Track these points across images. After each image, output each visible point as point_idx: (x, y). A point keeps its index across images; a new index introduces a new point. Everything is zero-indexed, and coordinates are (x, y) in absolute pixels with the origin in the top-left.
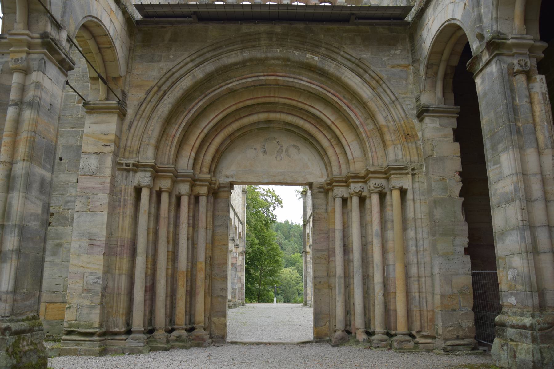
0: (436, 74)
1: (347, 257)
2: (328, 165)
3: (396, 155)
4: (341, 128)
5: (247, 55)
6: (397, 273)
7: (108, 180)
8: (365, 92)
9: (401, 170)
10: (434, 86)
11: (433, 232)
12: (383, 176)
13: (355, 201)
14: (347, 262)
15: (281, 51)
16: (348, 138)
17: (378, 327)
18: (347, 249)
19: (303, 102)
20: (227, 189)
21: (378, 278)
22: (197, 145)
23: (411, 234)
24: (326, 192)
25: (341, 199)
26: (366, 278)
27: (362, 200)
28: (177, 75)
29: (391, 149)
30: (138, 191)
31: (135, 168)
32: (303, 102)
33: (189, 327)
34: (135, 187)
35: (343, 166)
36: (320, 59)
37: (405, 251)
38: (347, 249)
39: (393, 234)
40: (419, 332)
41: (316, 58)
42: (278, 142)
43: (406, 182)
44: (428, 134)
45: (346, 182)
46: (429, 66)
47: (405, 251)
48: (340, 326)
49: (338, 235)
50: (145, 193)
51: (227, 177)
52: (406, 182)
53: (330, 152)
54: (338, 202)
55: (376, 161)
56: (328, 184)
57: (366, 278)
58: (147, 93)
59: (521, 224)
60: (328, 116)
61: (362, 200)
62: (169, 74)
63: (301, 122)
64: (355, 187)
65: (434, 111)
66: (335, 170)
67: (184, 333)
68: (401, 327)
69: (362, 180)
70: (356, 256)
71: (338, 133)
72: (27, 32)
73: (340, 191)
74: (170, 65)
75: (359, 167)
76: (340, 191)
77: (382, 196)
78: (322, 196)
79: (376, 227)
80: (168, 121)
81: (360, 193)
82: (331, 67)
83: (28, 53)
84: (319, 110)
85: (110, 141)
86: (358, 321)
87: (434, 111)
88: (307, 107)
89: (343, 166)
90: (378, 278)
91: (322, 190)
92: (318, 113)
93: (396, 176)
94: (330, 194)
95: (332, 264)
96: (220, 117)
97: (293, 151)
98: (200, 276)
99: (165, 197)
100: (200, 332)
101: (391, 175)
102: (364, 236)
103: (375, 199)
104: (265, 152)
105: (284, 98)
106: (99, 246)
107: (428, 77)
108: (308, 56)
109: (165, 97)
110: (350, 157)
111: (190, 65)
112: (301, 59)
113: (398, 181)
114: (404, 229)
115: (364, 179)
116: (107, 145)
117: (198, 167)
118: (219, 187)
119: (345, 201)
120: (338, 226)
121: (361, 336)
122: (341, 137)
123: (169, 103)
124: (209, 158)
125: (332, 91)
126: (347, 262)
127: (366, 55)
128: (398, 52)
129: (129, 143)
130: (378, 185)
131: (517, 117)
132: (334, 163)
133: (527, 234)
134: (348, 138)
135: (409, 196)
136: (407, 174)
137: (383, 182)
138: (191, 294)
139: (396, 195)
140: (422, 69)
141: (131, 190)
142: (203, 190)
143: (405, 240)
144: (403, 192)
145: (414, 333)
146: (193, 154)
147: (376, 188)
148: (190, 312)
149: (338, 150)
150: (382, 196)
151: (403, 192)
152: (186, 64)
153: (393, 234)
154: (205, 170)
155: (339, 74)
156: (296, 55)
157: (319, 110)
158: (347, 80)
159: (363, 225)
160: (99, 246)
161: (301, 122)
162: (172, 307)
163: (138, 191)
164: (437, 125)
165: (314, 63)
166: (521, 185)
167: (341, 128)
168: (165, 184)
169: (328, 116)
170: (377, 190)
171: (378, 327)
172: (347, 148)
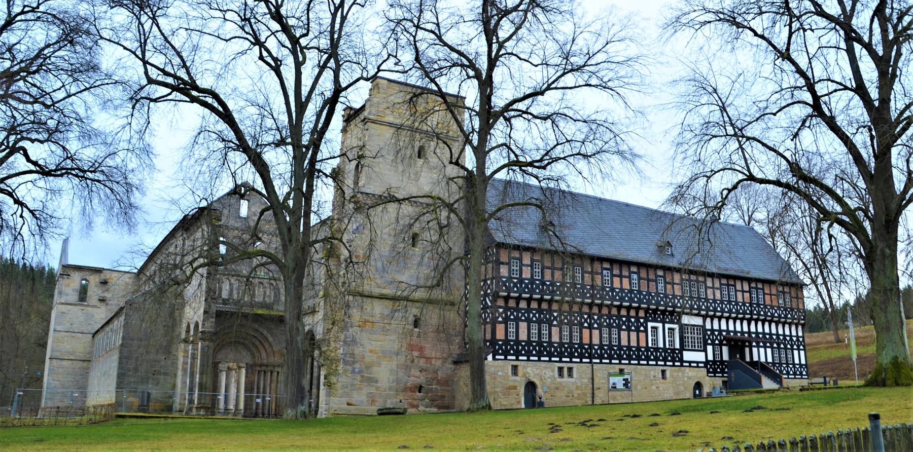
17: (266, 412)
23: (279, 385)
27: (265, 372)
37: (277, 389)
39: (273, 385)
43: (279, 370)
45: (261, 366)
47: (277, 389)
48: (254, 412)
49: (256, 383)
60: (257, 343)
61: (265, 372)
64: (263, 368)
68: (273, 412)
73: (258, 368)
75: (265, 362)
76: (258, 368)
77: (272, 372)
79: (269, 382)
82: (261, 330)
86: (260, 411)
102: (264, 384)
103: (269, 373)
113: (277, 369)
114: (277, 383)
115: (267, 366)
119: (259, 371)
120: (256, 380)
121: (261, 415)
139: (276, 373)
143: (277, 387)
144: (278, 372)
150: (272, 372)
151: (278, 372)
153: (273, 385)
159: (264, 381)
167: (261, 348)
169: (257, 343)
171: (266, 412)
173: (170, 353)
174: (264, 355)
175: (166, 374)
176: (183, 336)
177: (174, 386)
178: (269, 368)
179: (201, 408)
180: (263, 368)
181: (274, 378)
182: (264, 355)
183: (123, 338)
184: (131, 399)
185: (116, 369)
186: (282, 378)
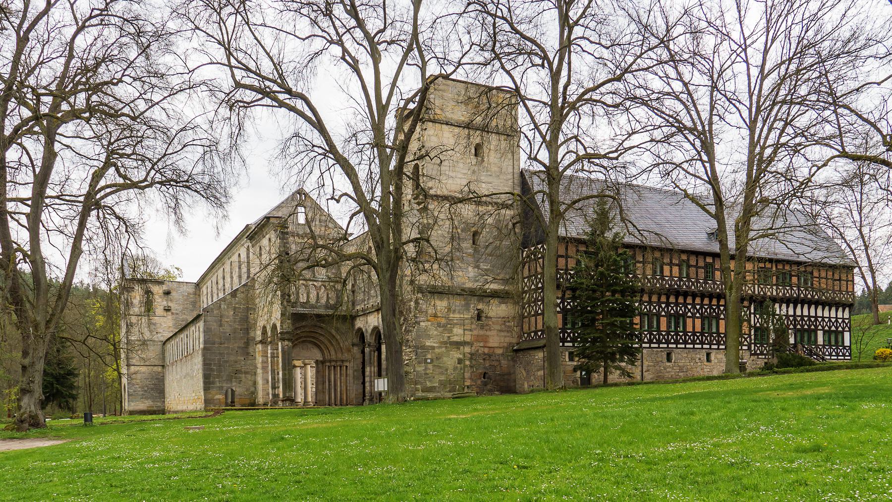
2: (323, 354)
4: (328, 345)
6: (344, 388)
9: (346, 361)
11: (354, 378)
14: (329, 385)
16: (331, 349)
18: (330, 381)
21: (339, 390)
26: (335, 390)
38: (330, 381)
43: (347, 364)
44: (355, 351)
45: (330, 361)
52: (347, 364)
57: (335, 390)
64: (333, 364)
73: (328, 364)
75: (334, 357)
86: (333, 401)
90: (339, 390)
115: (336, 361)
120: (327, 374)
126: (329, 385)
134: (331, 349)
140: (354, 332)
144: (347, 367)
150: (341, 367)
159: (335, 375)
173: (248, 354)
174: (333, 352)
175: (246, 373)
176: (259, 338)
177: (255, 383)
178: (338, 363)
179: (286, 400)
180: (333, 364)
181: (344, 372)
182: (333, 352)
183: (205, 342)
184: (218, 397)
185: (201, 371)
186: (350, 372)
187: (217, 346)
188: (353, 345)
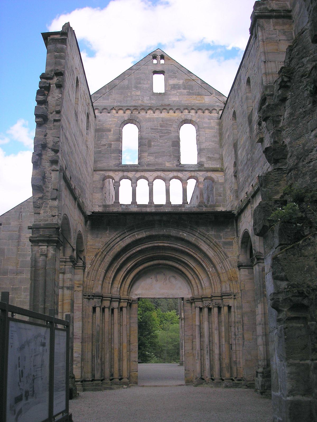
0: (247, 246)
1: (202, 339)
3: (226, 288)
5: (148, 233)
6: (225, 348)
7: (81, 305)
8: (210, 253)
10: (246, 252)
12: (220, 298)
13: (206, 310)
15: (166, 231)
16: (202, 276)
18: (201, 336)
19: (178, 256)
20: (137, 302)
22: (121, 281)
24: (191, 303)
25: (199, 309)
27: (210, 309)
28: (111, 245)
29: (224, 284)
30: (94, 309)
31: (92, 297)
32: (178, 256)
33: (120, 377)
34: (93, 307)
35: (200, 290)
36: (187, 235)
38: (201, 336)
40: (236, 378)
41: (185, 235)
42: (164, 274)
45: (201, 299)
46: (242, 243)
50: (98, 309)
51: (136, 295)
52: (231, 302)
53: (193, 282)
54: (198, 310)
55: (216, 290)
56: (192, 300)
58: (96, 256)
59: (262, 334)
60: (192, 264)
61: (210, 309)
62: (107, 245)
63: (177, 265)
64: (206, 303)
65: (245, 266)
66: (196, 292)
67: (118, 380)
69: (210, 299)
70: (206, 339)
71: (197, 272)
72: (65, 257)
74: (107, 239)
75: (208, 292)
76: (199, 304)
77: (219, 308)
78: (189, 305)
79: (215, 325)
80: (107, 271)
81: (208, 306)
82: (192, 239)
83: (65, 265)
84: (186, 259)
85: (80, 284)
87: (245, 266)
88: (180, 258)
89: (200, 290)
90: (217, 351)
91: (189, 302)
92: (186, 262)
93: (225, 299)
94: (193, 305)
95: (194, 343)
96: (133, 264)
97: (173, 280)
98: (125, 351)
99: (107, 310)
100: (125, 380)
101: (223, 299)
103: (216, 310)
104: (157, 281)
105: (168, 254)
106: (79, 338)
107: (242, 248)
108: (181, 233)
109: (106, 258)
110: (203, 286)
111: (118, 239)
112: (177, 235)
116: (79, 287)
117: (122, 292)
118: (133, 301)
119: (201, 309)
122: (199, 275)
123: (108, 261)
124: (127, 286)
125: (193, 251)
126: (201, 342)
127: (212, 233)
128: (229, 230)
129: (88, 284)
130: (217, 303)
131: (265, 289)
132: (195, 288)
133: (264, 338)
134: (202, 276)
135: (232, 309)
136: (231, 298)
137: (220, 301)
138: (120, 360)
139: (226, 309)
141: (91, 309)
142: (124, 304)
144: (229, 308)
145: (234, 378)
146: (119, 286)
147: (216, 305)
148: (120, 370)
149: (197, 281)
150: (219, 308)
151: (229, 308)
152: (116, 238)
154: (125, 293)
155: (197, 244)
156: (173, 232)
157: (186, 259)
158: (201, 247)
160: (79, 338)
161: (177, 265)
162: (112, 367)
163: (94, 309)
164: (247, 273)
165: (184, 237)
166: (263, 319)
167: (198, 270)
168: (107, 303)
169: (192, 264)
170: (217, 306)
172: (202, 281)
174: (205, 282)
180: (206, 303)
182: (205, 282)
187: (10, 276)
188: (240, 266)
